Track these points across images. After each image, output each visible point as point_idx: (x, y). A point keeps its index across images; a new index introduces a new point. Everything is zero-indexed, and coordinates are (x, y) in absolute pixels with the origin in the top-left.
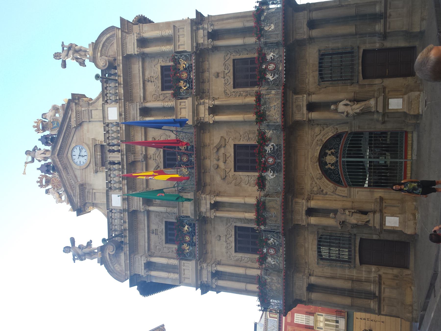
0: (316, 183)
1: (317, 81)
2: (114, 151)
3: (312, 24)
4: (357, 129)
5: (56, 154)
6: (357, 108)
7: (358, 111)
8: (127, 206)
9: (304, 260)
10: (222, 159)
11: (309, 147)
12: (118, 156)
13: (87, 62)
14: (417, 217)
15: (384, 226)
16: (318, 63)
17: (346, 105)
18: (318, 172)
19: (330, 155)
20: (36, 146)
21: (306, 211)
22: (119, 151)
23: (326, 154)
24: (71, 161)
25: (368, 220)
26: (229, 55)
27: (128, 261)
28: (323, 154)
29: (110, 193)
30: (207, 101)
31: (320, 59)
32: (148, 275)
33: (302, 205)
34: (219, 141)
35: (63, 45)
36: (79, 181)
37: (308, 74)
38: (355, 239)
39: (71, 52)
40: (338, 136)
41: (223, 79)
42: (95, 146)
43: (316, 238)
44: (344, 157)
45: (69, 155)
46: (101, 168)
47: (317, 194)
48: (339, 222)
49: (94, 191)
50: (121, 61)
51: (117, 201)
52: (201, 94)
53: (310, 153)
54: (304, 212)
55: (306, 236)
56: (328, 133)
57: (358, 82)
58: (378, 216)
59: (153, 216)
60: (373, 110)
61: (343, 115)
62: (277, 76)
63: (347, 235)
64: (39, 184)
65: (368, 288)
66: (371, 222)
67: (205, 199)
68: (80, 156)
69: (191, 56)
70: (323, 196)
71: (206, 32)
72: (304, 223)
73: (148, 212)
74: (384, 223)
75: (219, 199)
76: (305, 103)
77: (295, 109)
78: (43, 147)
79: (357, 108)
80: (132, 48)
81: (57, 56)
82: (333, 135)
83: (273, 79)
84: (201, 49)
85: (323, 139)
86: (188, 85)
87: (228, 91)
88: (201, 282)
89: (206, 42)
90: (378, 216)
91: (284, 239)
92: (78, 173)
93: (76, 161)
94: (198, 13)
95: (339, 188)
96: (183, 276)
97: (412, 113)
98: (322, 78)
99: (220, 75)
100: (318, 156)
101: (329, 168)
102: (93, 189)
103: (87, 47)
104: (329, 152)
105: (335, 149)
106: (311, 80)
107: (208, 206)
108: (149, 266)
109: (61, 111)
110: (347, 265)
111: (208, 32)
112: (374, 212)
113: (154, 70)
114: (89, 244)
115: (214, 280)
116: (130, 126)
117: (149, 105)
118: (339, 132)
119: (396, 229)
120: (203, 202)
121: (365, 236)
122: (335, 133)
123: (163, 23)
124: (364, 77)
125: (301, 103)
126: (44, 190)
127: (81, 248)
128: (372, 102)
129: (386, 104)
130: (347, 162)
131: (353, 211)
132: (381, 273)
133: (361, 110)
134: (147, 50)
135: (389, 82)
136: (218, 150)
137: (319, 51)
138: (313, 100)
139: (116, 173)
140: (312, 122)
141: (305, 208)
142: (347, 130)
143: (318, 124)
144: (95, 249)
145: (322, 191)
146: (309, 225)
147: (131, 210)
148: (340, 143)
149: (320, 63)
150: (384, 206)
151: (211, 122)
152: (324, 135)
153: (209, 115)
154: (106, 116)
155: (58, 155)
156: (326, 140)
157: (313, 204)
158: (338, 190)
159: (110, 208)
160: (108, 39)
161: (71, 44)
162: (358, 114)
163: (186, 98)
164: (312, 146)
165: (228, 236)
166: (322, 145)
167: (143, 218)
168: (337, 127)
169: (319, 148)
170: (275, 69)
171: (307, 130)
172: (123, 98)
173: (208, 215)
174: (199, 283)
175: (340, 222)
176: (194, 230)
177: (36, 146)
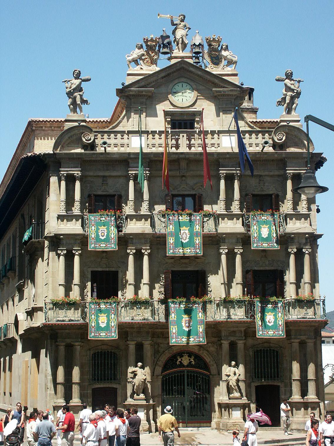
2: (189, 140)
5: (184, 66)
7: (230, 384)
17: (235, 374)
19: (189, 360)
20: (190, 29)
22: (190, 146)
23: (190, 356)
24: (176, 81)
31: (274, 350)
35: (299, 82)
40: (206, 367)
44: (188, 371)
45: (183, 79)
46: (170, 119)
58: (144, 402)
60: (231, 396)
73: (127, 178)
82: (208, 361)
88: (62, 239)
90: (144, 402)
93: (176, 87)
94: (320, 236)
95: (161, 368)
101: (177, 360)
102: (146, 108)
109: (229, 70)
110: (91, 377)
124: (257, 388)
126: (141, 42)
127: (81, 93)
128: (237, 394)
130: (184, 375)
155: (183, 68)
162: (228, 384)
163: (243, 225)
174: (61, 237)
175: (135, 372)
177: (190, 29)
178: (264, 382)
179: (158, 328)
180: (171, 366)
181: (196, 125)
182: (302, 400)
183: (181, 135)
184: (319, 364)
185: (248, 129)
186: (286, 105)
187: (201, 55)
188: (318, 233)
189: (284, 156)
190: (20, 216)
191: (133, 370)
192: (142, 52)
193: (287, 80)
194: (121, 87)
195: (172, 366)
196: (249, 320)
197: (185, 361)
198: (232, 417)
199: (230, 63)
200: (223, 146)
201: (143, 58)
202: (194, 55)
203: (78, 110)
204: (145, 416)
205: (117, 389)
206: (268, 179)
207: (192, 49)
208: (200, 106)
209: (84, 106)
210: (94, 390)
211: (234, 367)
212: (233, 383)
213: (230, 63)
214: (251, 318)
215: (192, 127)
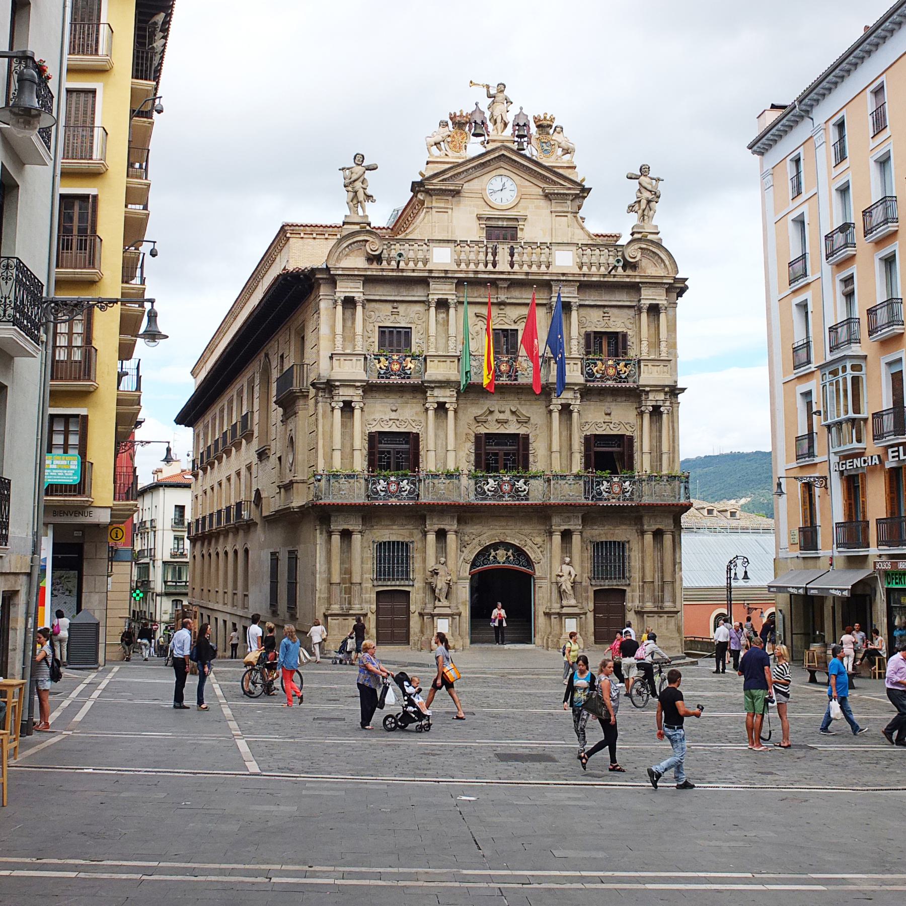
1: (594, 539)
3: (658, 535)
6: (567, 586)
7: (564, 587)
8: (437, 275)
10: (501, 417)
12: (506, 262)
13: (634, 219)
21: (444, 529)
22: (512, 266)
26: (630, 429)
27: (356, 273)
28: (508, 546)
29: (452, 245)
30: (578, 402)
32: (336, 301)
33: (451, 525)
34: (524, 413)
35: (658, 180)
36: (466, 186)
39: (647, 195)
40: (529, 563)
41: (602, 421)
42: (517, 220)
43: (407, 540)
49: (450, 211)
50: (633, 280)
51: (442, 258)
52: (586, 393)
53: (509, 531)
54: (442, 527)
59: (419, 308)
60: (565, 603)
64: (458, 114)
65: (356, 602)
66: (440, 604)
67: (451, 396)
68: (502, 191)
69: (634, 382)
71: (660, 403)
72: (428, 527)
75: (451, 414)
76: (571, 528)
78: (510, 118)
79: (567, 586)
80: (649, 296)
81: (644, 170)
84: (641, 396)
86: (598, 376)
87: (587, 427)
88: (338, 386)
89: (649, 403)
92: (475, 185)
93: (493, 181)
95: (469, 566)
96: (342, 359)
98: (598, 544)
99: (608, 417)
103: (654, 222)
104: (510, 553)
107: (442, 400)
108: (349, 303)
111: (660, 406)
113: (618, 323)
114: (369, 197)
115: (342, 405)
116: (546, 285)
117: (574, 314)
120: (448, 392)
123: (675, 338)
125: (572, 523)
128: (573, 602)
132: (369, 615)
133: (564, 591)
134: (644, 316)
135: (590, 616)
136: (513, 413)
138: (574, 537)
139: (482, 256)
141: (447, 528)
142: (538, 574)
144: (364, 211)
146: (425, 534)
147: (430, 280)
149: (615, 542)
151: (551, 407)
153: (561, 404)
154: (560, 248)
155: (503, 155)
157: (451, 538)
159: (430, 244)
160: (662, 261)
161: (658, 197)
162: (560, 587)
163: (582, 374)
165: (398, 423)
167: (418, 294)
169: (516, 542)
172: (586, 279)
173: (430, 399)
174: (337, 383)
176: (409, 378)
178: (607, 584)
181: (520, 234)
182: (656, 609)
183: (500, 247)
184: (678, 561)
185: (590, 242)
186: (640, 212)
187: (526, 139)
188: (679, 386)
189: (638, 280)
190: (263, 354)
192: (445, 131)
193: (642, 178)
194: (419, 179)
196: (590, 502)
199: (567, 151)
200: (557, 264)
201: (449, 139)
202: (516, 139)
203: (360, 209)
206: (615, 311)
207: (514, 131)
208: (526, 208)
209: (368, 205)
210: (378, 593)
211: (568, 564)
213: (567, 151)
215: (514, 237)
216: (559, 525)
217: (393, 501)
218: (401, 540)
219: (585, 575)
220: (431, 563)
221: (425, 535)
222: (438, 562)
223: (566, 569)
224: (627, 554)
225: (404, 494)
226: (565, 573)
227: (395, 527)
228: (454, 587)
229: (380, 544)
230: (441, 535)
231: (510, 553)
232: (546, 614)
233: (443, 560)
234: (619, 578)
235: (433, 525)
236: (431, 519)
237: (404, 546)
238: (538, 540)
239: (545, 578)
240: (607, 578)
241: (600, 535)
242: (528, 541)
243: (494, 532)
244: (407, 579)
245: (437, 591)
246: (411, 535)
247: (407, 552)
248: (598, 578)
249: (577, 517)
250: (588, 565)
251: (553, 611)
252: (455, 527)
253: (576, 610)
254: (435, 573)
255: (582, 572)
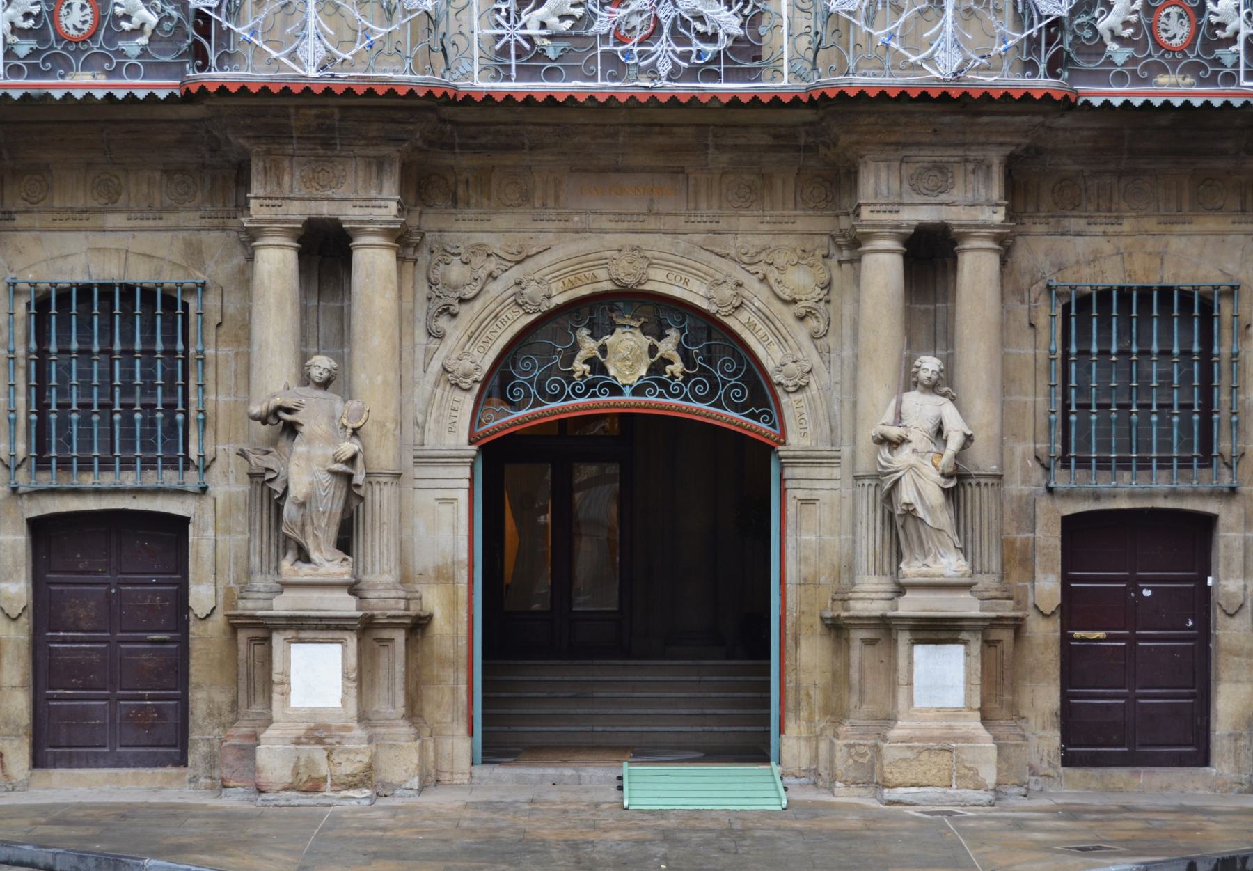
0: (491, 277)
4: (801, 494)
9: (21, 204)
11: (698, 238)
14: (350, 793)
15: (290, 634)
16: (1168, 281)
17: (939, 432)
18: (555, 288)
19: (653, 350)
25: (314, 555)
28: (657, 311)
37: (1111, 229)
38: (180, 492)
40: (758, 391)
43: (170, 278)
47: (432, 284)
48: (290, 403)
53: (663, 242)
54: (325, 210)
55: (171, 219)
56: (782, 340)
57: (1050, 490)
60: (911, 570)
61: (889, 416)
62: (1118, 53)
63: (202, 448)
66: (304, 572)
70: (421, 315)
74: (303, 635)
76: (954, 216)
77: (927, 156)
82: (769, 366)
83: (1107, 37)
85: (744, 316)
91: (162, 94)
95: (468, 402)
97: (891, 752)
98: (1084, 301)
100: (648, 287)
101: (576, 348)
104: (667, 347)
105: (687, 377)
106: (1080, 246)
110: (21, 448)
112: (353, 589)
118: (784, 400)
119: (276, 697)
121: (201, 542)
122: (776, 378)
124: (1071, 525)
125: (956, 194)
128: (950, 565)
129: (937, 630)
131: (359, 478)
133: (910, 512)
137: (1232, 291)
140: (846, 254)
141: (349, 214)
142: (797, 439)
143: (828, 286)
145: (446, 311)
146: (250, 240)
148: (718, 405)
149: (1166, 292)
150: (385, 634)
152: (766, 319)
156: (737, 327)
157: (373, 263)
158: (459, 395)
164: (706, 255)
166: (713, 309)
168: (813, 385)
169: (695, 293)
170: (1158, 45)
171: (800, 225)
175: (289, 411)
178: (1124, 492)
179: (451, 147)
180: (533, 391)
191: (278, 401)
195: (541, 391)
197: (627, 352)
198: (911, 702)
204: (345, 692)
205: (183, 522)
211: (932, 388)
212: (922, 486)
214: (1052, 72)
216: (892, 201)
217: (84, 82)
218: (140, 274)
219: (1022, 449)
220: (275, 378)
221: (251, 258)
222: (305, 379)
223: (922, 409)
224: (1222, 349)
225: (133, 47)
226: (918, 433)
227: (115, 220)
228: (382, 499)
229: (42, 304)
230: (325, 254)
231: (667, 347)
232: (837, 628)
233: (321, 364)
234: (1185, 463)
235: (282, 202)
236: (274, 171)
237: (161, 308)
238: (800, 281)
239: (830, 460)
240: (1124, 464)
241: (1094, 259)
242: (752, 284)
243: (588, 244)
244: (171, 463)
245: (289, 510)
246: (195, 254)
247: (170, 338)
248: (1083, 463)
249: (982, 167)
250: (1038, 398)
251: (859, 608)
252: (388, 211)
253: (965, 606)
254: (284, 424)
255: (1007, 431)
